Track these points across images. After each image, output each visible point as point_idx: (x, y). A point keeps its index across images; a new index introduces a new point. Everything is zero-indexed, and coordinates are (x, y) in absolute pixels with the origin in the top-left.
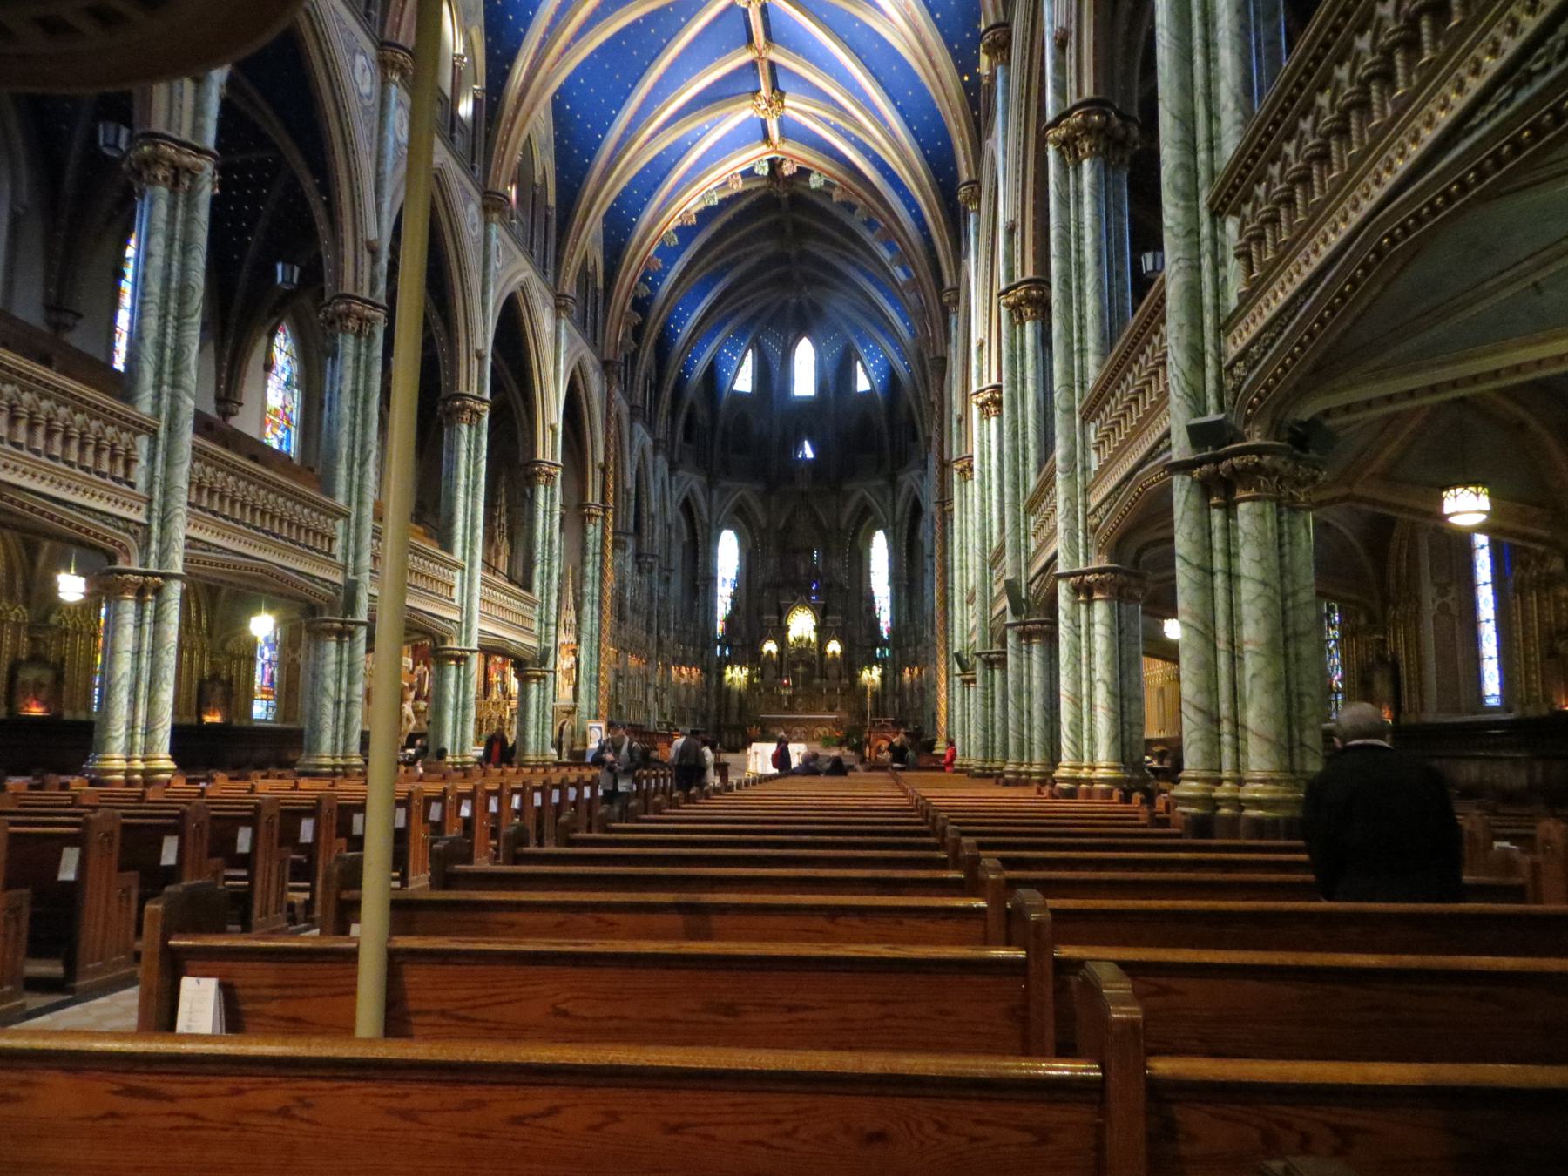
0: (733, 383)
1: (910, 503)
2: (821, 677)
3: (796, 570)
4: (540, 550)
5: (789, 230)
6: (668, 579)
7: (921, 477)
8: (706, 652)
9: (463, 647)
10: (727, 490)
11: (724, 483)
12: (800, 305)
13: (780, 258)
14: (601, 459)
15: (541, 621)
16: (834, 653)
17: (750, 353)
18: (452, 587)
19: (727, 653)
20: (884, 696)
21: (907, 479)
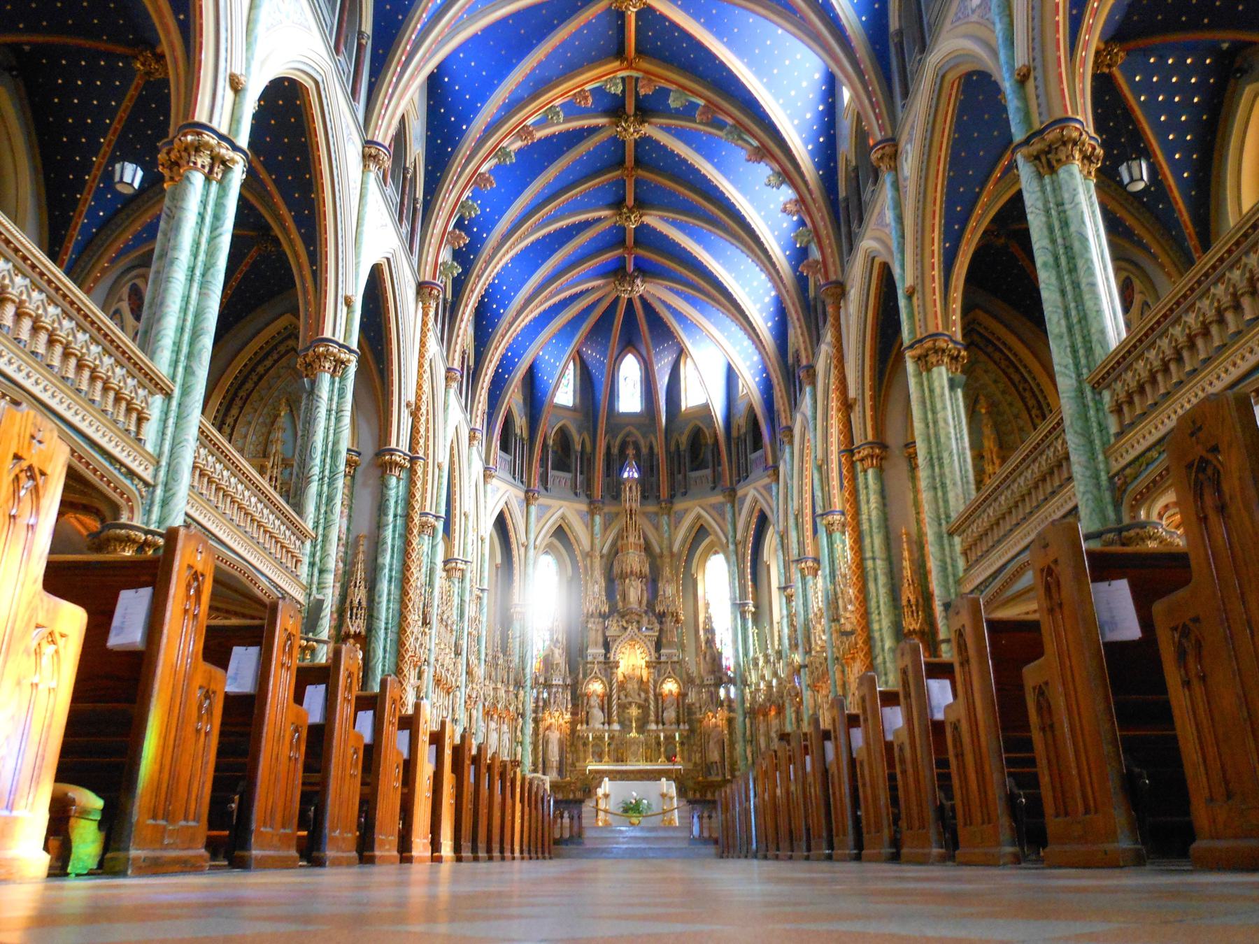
0: (554, 395)
1: (754, 520)
2: (657, 723)
3: (624, 597)
4: (318, 461)
5: (630, 200)
6: (479, 598)
7: (768, 488)
8: (522, 693)
9: (153, 527)
10: (549, 507)
11: (542, 500)
12: (630, 301)
13: (617, 238)
14: (412, 398)
15: (312, 564)
16: (671, 692)
17: (571, 365)
18: (141, 420)
19: (545, 695)
20: (732, 744)
21: (750, 492)
